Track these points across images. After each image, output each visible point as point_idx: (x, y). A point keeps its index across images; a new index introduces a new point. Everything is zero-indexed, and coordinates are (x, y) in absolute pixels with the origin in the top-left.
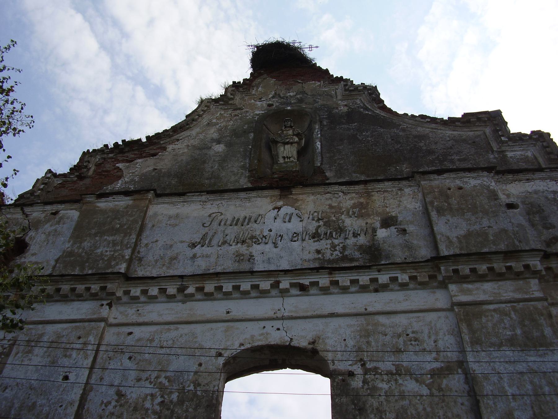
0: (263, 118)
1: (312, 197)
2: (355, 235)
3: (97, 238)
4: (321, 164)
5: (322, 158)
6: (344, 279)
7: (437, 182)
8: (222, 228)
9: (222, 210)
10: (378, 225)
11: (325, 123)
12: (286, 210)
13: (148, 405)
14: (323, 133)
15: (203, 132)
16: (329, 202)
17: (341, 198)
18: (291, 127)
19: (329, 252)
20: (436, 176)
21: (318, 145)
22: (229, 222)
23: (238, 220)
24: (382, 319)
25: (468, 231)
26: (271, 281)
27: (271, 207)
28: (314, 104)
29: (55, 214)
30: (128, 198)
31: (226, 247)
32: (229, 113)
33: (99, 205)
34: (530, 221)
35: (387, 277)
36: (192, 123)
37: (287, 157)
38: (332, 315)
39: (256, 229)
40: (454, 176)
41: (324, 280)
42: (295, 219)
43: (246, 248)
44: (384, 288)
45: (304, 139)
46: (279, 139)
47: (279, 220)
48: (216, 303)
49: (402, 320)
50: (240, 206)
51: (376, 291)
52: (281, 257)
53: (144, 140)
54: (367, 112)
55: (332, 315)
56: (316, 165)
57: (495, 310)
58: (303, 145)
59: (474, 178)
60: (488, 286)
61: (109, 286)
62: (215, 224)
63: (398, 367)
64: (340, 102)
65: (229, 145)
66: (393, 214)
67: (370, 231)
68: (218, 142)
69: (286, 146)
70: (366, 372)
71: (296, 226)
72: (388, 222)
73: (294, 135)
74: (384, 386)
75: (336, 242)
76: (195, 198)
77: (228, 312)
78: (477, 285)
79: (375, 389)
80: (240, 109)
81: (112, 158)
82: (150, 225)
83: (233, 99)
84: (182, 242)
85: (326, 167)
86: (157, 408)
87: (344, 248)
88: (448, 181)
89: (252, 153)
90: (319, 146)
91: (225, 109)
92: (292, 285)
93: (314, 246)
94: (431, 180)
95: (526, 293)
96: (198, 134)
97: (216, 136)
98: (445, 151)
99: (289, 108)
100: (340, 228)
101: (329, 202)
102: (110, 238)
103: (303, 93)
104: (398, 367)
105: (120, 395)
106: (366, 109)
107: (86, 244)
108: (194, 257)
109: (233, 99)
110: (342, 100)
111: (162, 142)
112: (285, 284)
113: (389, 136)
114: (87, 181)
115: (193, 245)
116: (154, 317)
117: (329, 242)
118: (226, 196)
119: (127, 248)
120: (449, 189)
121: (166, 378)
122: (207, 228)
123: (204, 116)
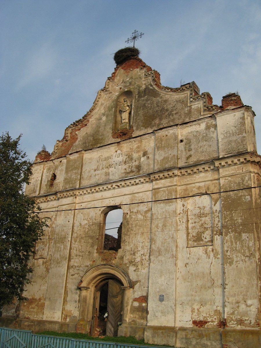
0: (118, 97)
1: (126, 145)
2: (135, 161)
3: (71, 172)
4: (133, 123)
5: (133, 119)
6: (128, 182)
7: (160, 133)
8: (102, 162)
9: (102, 154)
10: (142, 156)
11: (137, 98)
12: (119, 152)
13: (86, 227)
15: (100, 109)
16: (130, 146)
17: (133, 144)
19: (128, 169)
20: (160, 131)
22: (104, 160)
23: (106, 158)
24: (136, 195)
25: (164, 157)
26: (111, 185)
27: (114, 151)
28: (134, 85)
29: (61, 162)
30: (77, 154)
31: (103, 170)
32: (108, 96)
33: (71, 157)
34: (185, 148)
35: (138, 180)
36: (96, 106)
38: (125, 195)
39: (111, 161)
40: (166, 130)
41: (123, 183)
42: (121, 156)
43: (108, 170)
44: (137, 184)
47: (116, 157)
48: (99, 193)
49: (141, 195)
50: (107, 151)
51: (136, 185)
52: (116, 173)
53: (82, 118)
54: (151, 88)
55: (125, 195)
57: (162, 190)
59: (172, 129)
60: (163, 181)
61: (74, 192)
62: (100, 160)
63: (138, 210)
65: (107, 117)
66: (147, 150)
67: (139, 159)
68: (104, 115)
70: (131, 212)
71: (121, 159)
72: (145, 154)
73: (127, 106)
74: (134, 217)
75: (130, 164)
76: (95, 150)
77: (102, 196)
78: (160, 181)
79: (132, 218)
80: (111, 93)
81: (74, 129)
82: (84, 164)
83: (108, 88)
84: (92, 169)
86: (88, 227)
87: (132, 167)
88: (164, 132)
90: (133, 113)
91: (106, 94)
92: (116, 185)
93: (124, 167)
94: (158, 133)
95: (172, 183)
96: (98, 111)
97: (103, 111)
98: (172, 108)
99: (126, 90)
100: (132, 158)
101: (130, 146)
102: (74, 171)
103: (132, 78)
104: (138, 210)
105: (80, 224)
106: (151, 86)
107: (69, 175)
108: (95, 175)
109: (108, 88)
110: (144, 81)
111: (88, 118)
112: (114, 186)
113: (156, 102)
114: (69, 141)
115: (95, 170)
116: (86, 200)
117: (128, 165)
118: (103, 148)
119: (79, 175)
120: (163, 136)
121: (89, 218)
122: (98, 163)
123: (100, 100)
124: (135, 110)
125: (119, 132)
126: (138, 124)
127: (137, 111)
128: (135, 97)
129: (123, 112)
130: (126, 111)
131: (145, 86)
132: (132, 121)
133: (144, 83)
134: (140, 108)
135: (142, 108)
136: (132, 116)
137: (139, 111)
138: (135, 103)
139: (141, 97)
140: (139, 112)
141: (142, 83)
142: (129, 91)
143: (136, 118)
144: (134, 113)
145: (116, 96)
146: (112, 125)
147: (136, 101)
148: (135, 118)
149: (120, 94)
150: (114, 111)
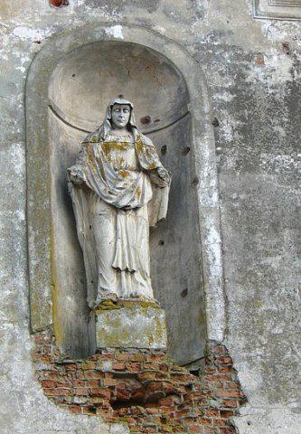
4: (226, 332)
5: (227, 302)
14: (223, 183)
18: (129, 128)
21: (213, 242)
28: (188, 23)
37: (127, 270)
45: (167, 189)
46: (101, 187)
56: (210, 338)
58: (164, 214)
64: (267, 24)
69: (121, 218)
73: (139, 169)
85: (236, 345)
89: (32, 247)
99: (117, 32)
110: (275, 18)
124: (229, 230)
125: (107, 365)
126: (278, 355)
127: (246, 246)
128: (216, 124)
129: (99, 207)
130: (136, 209)
131: (287, 63)
132: (220, 314)
133: (283, 36)
134: (275, 227)
135: (287, 234)
136: (216, 270)
137: (267, 254)
138: (219, 171)
139: (270, 142)
140: (274, 262)
141: (261, 38)
142: (146, 50)
143: (251, 304)
144: (223, 252)
145: (21, 46)
146: (21, 283)
147: (230, 163)
148: (240, 293)
149: (65, 44)
150: (19, 168)
